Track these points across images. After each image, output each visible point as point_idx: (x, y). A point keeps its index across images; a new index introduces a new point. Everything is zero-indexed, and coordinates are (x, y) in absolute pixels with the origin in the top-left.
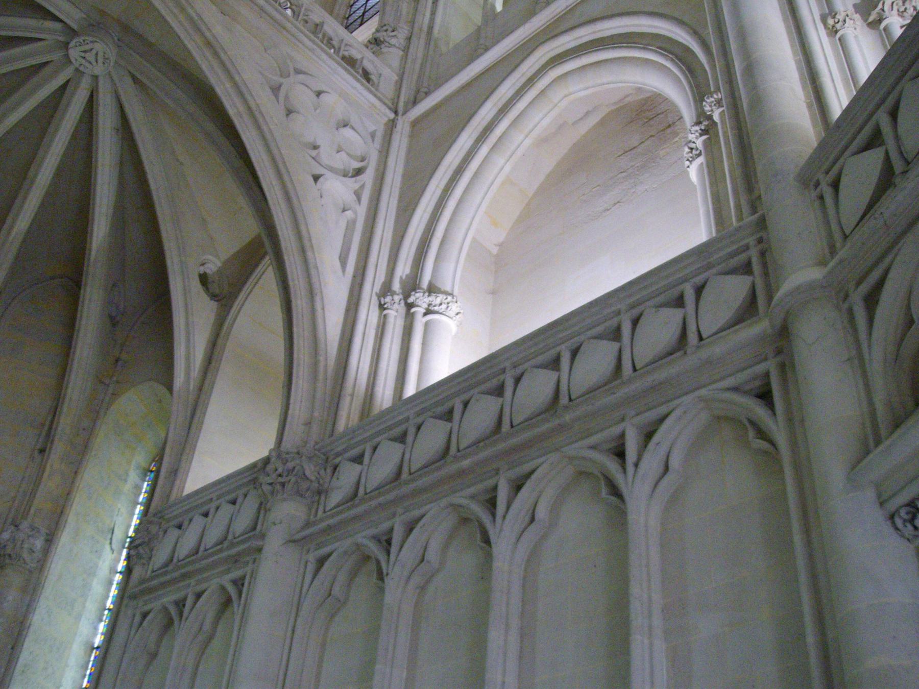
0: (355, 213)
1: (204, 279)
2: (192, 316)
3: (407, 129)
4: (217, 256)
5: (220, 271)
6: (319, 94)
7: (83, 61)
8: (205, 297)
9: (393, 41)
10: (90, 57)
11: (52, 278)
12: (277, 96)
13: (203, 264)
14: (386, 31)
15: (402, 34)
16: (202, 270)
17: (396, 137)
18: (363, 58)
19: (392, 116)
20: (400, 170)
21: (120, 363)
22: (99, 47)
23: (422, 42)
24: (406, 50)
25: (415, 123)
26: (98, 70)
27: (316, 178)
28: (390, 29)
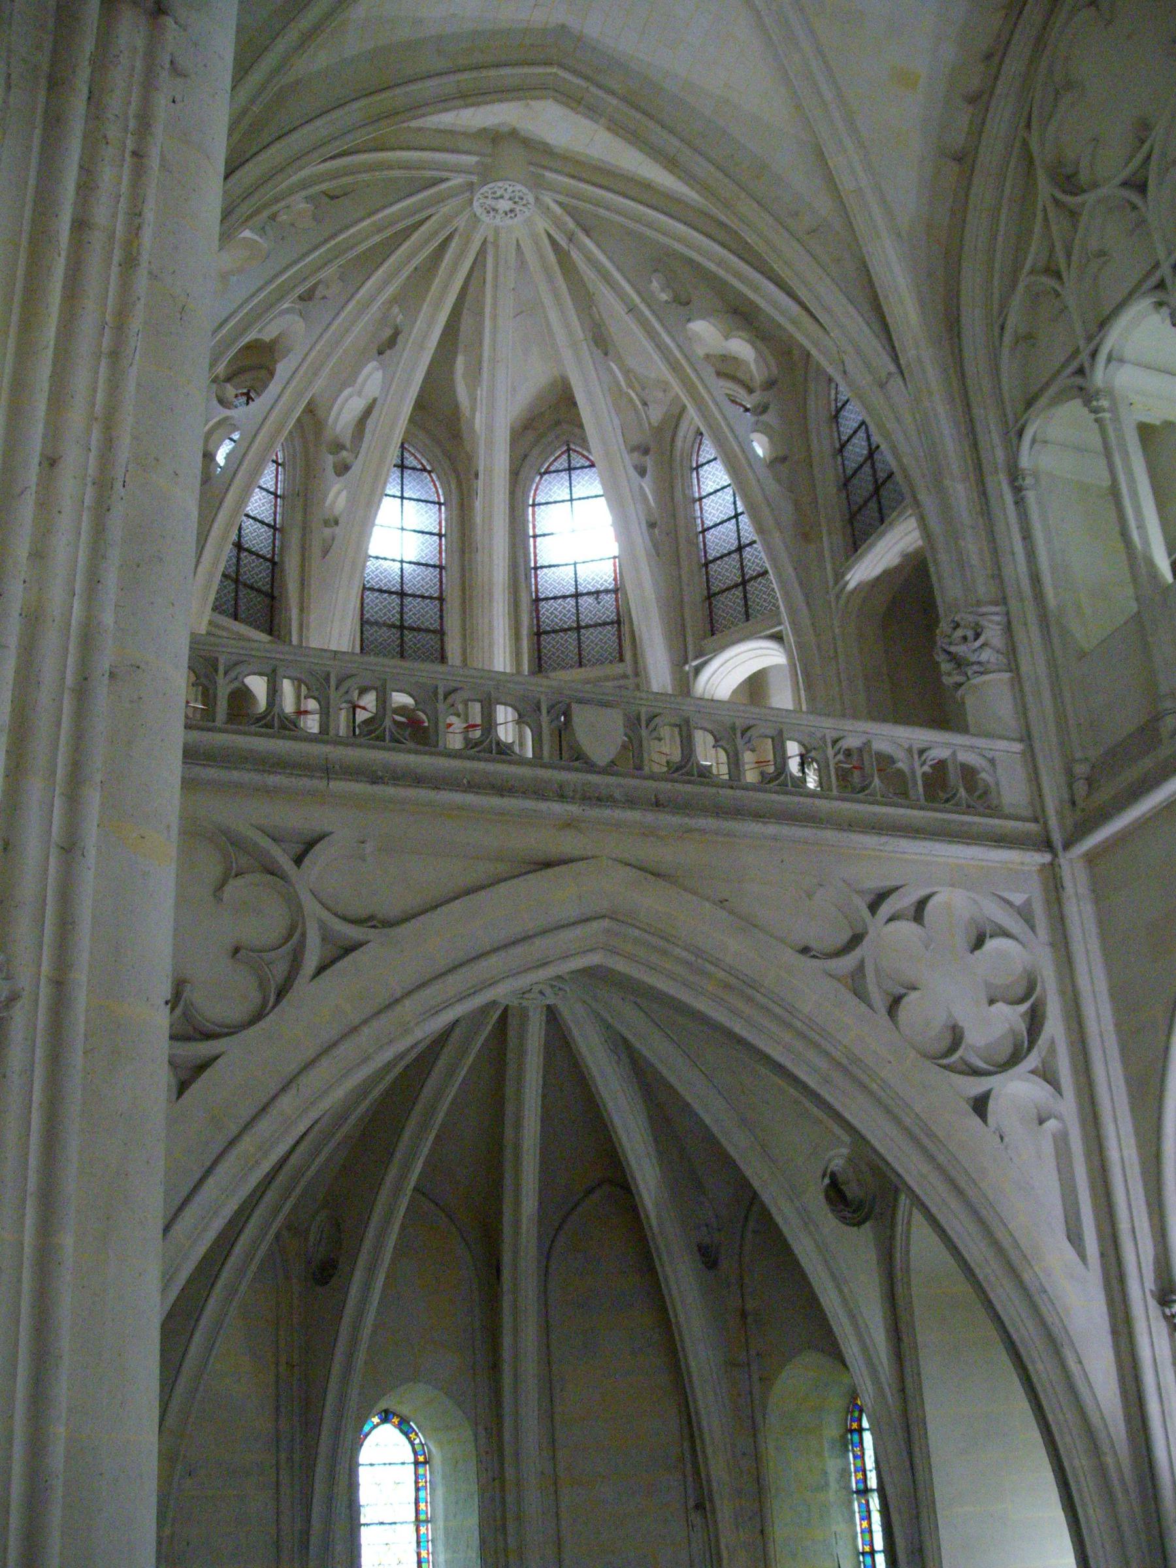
0: (1059, 1117)
2: (838, 1266)
3: (1082, 876)
6: (919, 912)
9: (985, 656)
11: (590, 1191)
12: (860, 994)
14: (965, 638)
15: (993, 634)
17: (1072, 909)
18: (954, 754)
19: (1047, 858)
20: (1102, 986)
21: (750, 1319)
23: (1034, 630)
24: (1012, 664)
25: (1091, 859)
27: (980, 1105)
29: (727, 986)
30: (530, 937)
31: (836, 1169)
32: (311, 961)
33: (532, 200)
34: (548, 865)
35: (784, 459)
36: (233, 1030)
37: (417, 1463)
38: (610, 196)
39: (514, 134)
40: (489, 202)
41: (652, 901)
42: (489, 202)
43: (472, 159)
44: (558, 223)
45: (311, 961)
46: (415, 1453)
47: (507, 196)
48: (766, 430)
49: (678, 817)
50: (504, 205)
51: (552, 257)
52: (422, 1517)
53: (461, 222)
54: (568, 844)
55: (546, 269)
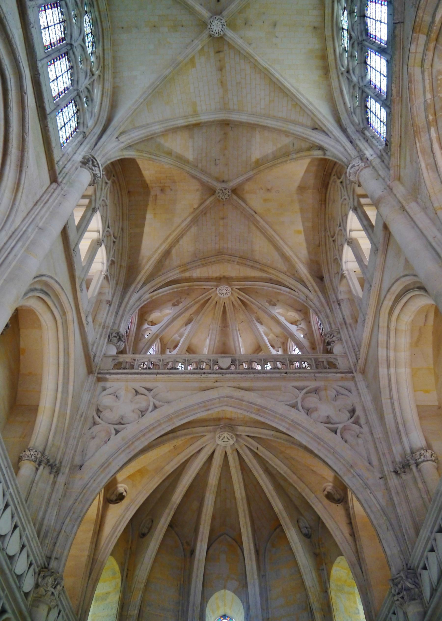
1: (329, 496)
4: (328, 481)
5: (334, 487)
7: (224, 443)
8: (334, 505)
10: (226, 440)
13: (325, 490)
16: (326, 493)
22: (226, 435)
26: (231, 442)
28: (329, 335)
29: (259, 410)
31: (329, 491)
32: (150, 409)
33: (230, 289)
35: (306, 334)
38: (246, 282)
39: (224, 277)
40: (221, 292)
42: (221, 292)
43: (215, 283)
44: (239, 294)
45: (150, 409)
47: (224, 289)
48: (302, 329)
50: (224, 292)
51: (240, 303)
53: (213, 295)
55: (240, 306)
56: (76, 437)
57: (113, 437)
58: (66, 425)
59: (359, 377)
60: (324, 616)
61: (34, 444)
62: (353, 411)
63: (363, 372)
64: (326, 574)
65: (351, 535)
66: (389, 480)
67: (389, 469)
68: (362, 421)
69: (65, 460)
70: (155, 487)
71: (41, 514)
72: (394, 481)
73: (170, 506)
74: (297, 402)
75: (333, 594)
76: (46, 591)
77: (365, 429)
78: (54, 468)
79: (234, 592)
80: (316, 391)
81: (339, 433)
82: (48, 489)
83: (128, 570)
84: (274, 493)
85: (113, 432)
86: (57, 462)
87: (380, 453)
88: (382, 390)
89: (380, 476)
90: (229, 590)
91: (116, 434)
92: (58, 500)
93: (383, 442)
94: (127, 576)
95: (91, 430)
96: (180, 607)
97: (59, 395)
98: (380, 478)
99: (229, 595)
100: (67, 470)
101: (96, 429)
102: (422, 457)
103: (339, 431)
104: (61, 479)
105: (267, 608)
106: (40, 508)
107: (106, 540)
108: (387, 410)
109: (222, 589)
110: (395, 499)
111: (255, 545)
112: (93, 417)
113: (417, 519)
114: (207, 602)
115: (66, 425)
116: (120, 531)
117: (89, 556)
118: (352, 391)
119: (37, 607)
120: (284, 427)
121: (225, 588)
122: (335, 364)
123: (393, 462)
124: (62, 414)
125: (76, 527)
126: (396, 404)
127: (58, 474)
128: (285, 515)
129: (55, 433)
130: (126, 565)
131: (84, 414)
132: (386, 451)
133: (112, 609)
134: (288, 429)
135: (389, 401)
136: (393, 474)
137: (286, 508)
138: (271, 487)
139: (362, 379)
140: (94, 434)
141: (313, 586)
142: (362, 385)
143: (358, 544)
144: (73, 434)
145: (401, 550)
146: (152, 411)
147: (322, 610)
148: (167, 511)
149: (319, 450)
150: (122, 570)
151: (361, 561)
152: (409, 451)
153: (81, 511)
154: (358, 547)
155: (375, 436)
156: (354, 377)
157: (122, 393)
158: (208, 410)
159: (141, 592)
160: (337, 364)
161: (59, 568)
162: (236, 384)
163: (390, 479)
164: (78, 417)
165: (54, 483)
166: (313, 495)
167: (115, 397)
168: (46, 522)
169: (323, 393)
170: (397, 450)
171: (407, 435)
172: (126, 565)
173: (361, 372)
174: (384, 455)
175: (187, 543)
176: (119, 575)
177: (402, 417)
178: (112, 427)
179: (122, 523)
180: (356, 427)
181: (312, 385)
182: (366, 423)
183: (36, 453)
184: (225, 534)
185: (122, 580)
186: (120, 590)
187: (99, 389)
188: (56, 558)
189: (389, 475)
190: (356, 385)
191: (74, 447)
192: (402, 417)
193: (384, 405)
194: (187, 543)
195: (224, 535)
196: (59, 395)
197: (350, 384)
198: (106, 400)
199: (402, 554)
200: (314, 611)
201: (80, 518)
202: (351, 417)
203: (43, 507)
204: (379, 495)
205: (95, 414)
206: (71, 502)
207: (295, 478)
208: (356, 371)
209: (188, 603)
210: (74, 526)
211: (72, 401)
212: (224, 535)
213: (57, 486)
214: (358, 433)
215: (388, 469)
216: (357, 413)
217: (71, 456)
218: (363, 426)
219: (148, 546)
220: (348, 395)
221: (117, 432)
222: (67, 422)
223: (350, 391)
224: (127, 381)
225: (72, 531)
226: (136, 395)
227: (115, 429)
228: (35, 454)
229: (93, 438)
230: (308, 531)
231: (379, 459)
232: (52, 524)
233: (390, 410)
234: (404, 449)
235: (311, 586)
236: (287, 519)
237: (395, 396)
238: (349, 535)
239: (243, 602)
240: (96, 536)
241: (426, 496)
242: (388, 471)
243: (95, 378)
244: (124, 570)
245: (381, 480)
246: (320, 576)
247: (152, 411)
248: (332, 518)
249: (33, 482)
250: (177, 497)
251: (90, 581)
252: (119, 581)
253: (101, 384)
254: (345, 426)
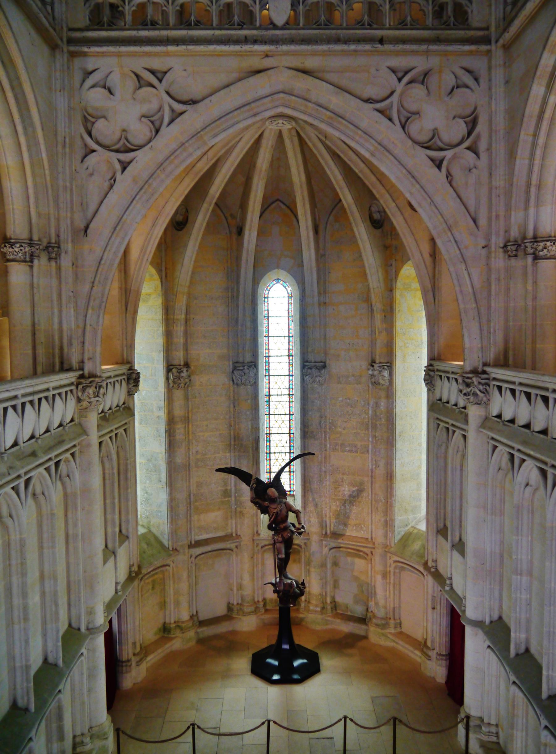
30: (249, 104)
34: (259, 72)
36: (140, 147)
37: (289, 297)
41: (302, 84)
45: (166, 120)
46: (288, 293)
49: (310, 46)
52: (290, 315)
54: (268, 63)
56: (66, 187)
57: (118, 175)
58: (48, 178)
59: (498, 54)
60: (385, 316)
61: (14, 232)
62: (472, 123)
63: (506, 48)
64: (394, 271)
65: (431, 256)
66: (493, 259)
67: (498, 243)
68: (482, 146)
69: (62, 230)
70: (186, 192)
71: (56, 320)
72: (499, 261)
73: (208, 199)
74: (392, 103)
75: (398, 294)
76: (89, 403)
77: (484, 161)
78: (53, 250)
79: (289, 272)
80: (423, 78)
81: (444, 169)
82: (54, 282)
83: (166, 268)
84: (343, 183)
85: (118, 167)
86: (53, 241)
87: (494, 214)
88: (525, 119)
89: (483, 243)
90: (283, 269)
91: (124, 169)
92: (71, 294)
93: (502, 196)
94: (166, 276)
95: (85, 165)
96: (230, 294)
97: (22, 139)
98: (483, 247)
99: (282, 274)
100: (70, 245)
101: (92, 159)
102: (545, 251)
103: (445, 163)
104: (66, 262)
105: (325, 292)
106: (53, 313)
107: (136, 265)
108: (523, 151)
109: (275, 269)
110: (493, 287)
111: (314, 220)
112: (82, 137)
113: (511, 323)
114: (258, 283)
115: (48, 178)
116: (150, 252)
117: (121, 288)
118: (481, 81)
119: (86, 417)
120: (367, 150)
121: (278, 267)
122: (466, 12)
123: (506, 232)
124: (36, 163)
125: (101, 316)
126: (538, 153)
127: (60, 255)
128: (354, 208)
129: (36, 194)
130: (164, 264)
131: (67, 140)
132: (502, 213)
133: (156, 313)
134: (373, 154)
135: (530, 139)
136: (501, 250)
137: (356, 200)
138: (340, 177)
139: (502, 63)
140: (90, 170)
141: (378, 287)
142: (499, 75)
143: (437, 268)
144: (61, 183)
145: (482, 347)
146: (169, 124)
147: (384, 310)
148: (205, 205)
149: (411, 193)
150: (159, 271)
151: (436, 290)
152: (530, 234)
153: (103, 295)
154: (437, 271)
155: (494, 183)
156: (489, 52)
157: (115, 80)
158: (255, 115)
159: (185, 297)
160: (469, 11)
161: (96, 368)
162: (297, 62)
163: (495, 258)
164: (60, 149)
165: (59, 268)
166: (394, 204)
167: (106, 92)
168: (65, 327)
169: (433, 80)
170: (517, 217)
171: (538, 205)
172: (164, 264)
173: (504, 46)
174: (497, 217)
175: (232, 215)
176: (156, 277)
177: (541, 175)
178: (114, 156)
179: (152, 242)
180: (470, 155)
181: (420, 63)
182: (488, 150)
183: (22, 248)
184: (278, 200)
185: (162, 282)
186: (161, 294)
187: (78, 76)
188: (90, 359)
189: (496, 252)
190: (490, 68)
191: (69, 205)
192: (541, 175)
193: (521, 144)
194: (232, 215)
195: (279, 202)
196: (22, 139)
197: (479, 64)
198: (95, 98)
199: (482, 352)
200: (375, 313)
201: (104, 304)
202: (468, 137)
203: (56, 310)
204: (476, 274)
205: (82, 130)
206: (87, 287)
207: (373, 178)
208: (497, 41)
209: (238, 291)
210: (99, 316)
211: (44, 135)
212: (279, 202)
213: (63, 274)
214: (472, 165)
215: (497, 241)
216: (479, 128)
217: (69, 222)
218: (482, 155)
219: (186, 246)
220: (473, 87)
221: (124, 166)
222: (47, 172)
223: (476, 79)
224: (119, 55)
225: (98, 322)
226: (140, 87)
227: (119, 161)
228: (21, 250)
229: (91, 175)
230: (381, 216)
231: (490, 219)
232: (73, 327)
233: (528, 151)
234: (526, 225)
235: (375, 287)
236: (357, 215)
237: (541, 140)
238: (428, 256)
239: (298, 283)
240: (123, 272)
241: (531, 303)
242: (496, 244)
243: (66, 55)
244: (161, 270)
245: (485, 249)
246: (386, 272)
247: (169, 124)
248: (413, 234)
249: (32, 286)
250: (216, 189)
251: (128, 315)
252: (158, 283)
253: (78, 62)
254: (455, 153)
